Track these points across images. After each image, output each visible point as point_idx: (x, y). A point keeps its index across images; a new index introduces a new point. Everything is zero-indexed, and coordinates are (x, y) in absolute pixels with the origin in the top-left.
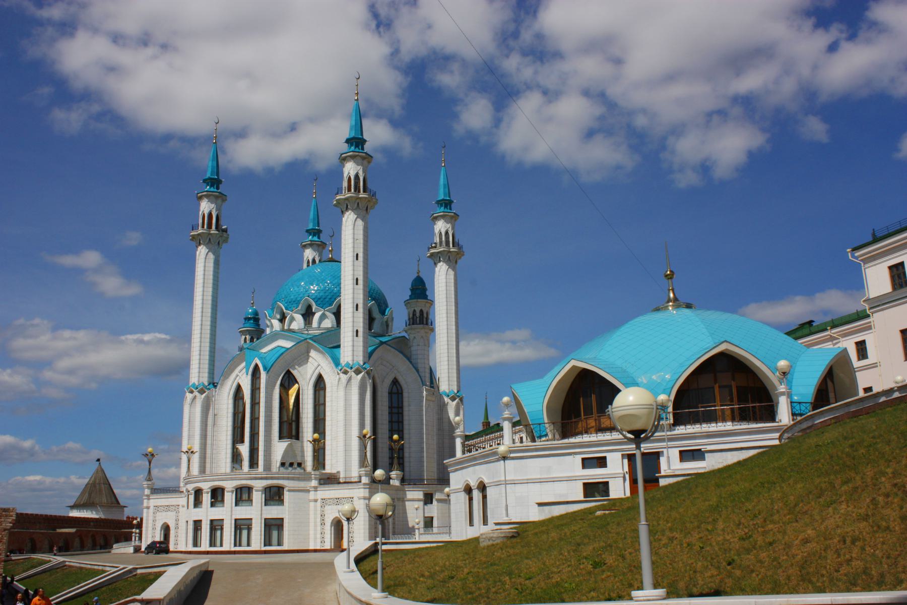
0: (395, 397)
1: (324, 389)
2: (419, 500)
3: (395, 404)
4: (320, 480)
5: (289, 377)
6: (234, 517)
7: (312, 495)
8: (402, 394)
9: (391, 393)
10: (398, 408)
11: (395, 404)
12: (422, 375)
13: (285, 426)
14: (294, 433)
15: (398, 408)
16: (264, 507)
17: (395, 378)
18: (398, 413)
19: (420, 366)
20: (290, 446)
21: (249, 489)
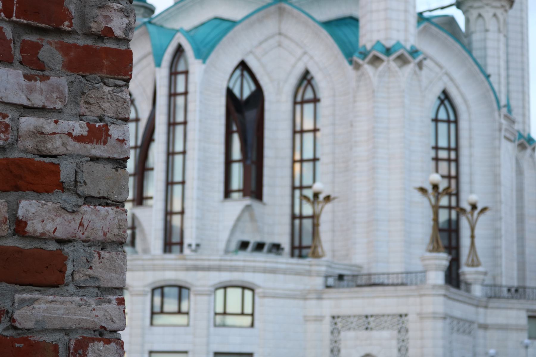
0: (443, 127)
1: (315, 100)
2: (518, 329)
3: (443, 143)
4: (327, 277)
5: (242, 75)
6: (149, 347)
7: (313, 307)
8: (456, 122)
9: (436, 120)
10: (449, 149)
11: (443, 143)
12: (496, 87)
13: (237, 170)
14: (253, 186)
15: (449, 149)
16: (212, 329)
17: (445, 92)
18: (449, 160)
19: (490, 70)
20: (248, 207)
21: (182, 290)
